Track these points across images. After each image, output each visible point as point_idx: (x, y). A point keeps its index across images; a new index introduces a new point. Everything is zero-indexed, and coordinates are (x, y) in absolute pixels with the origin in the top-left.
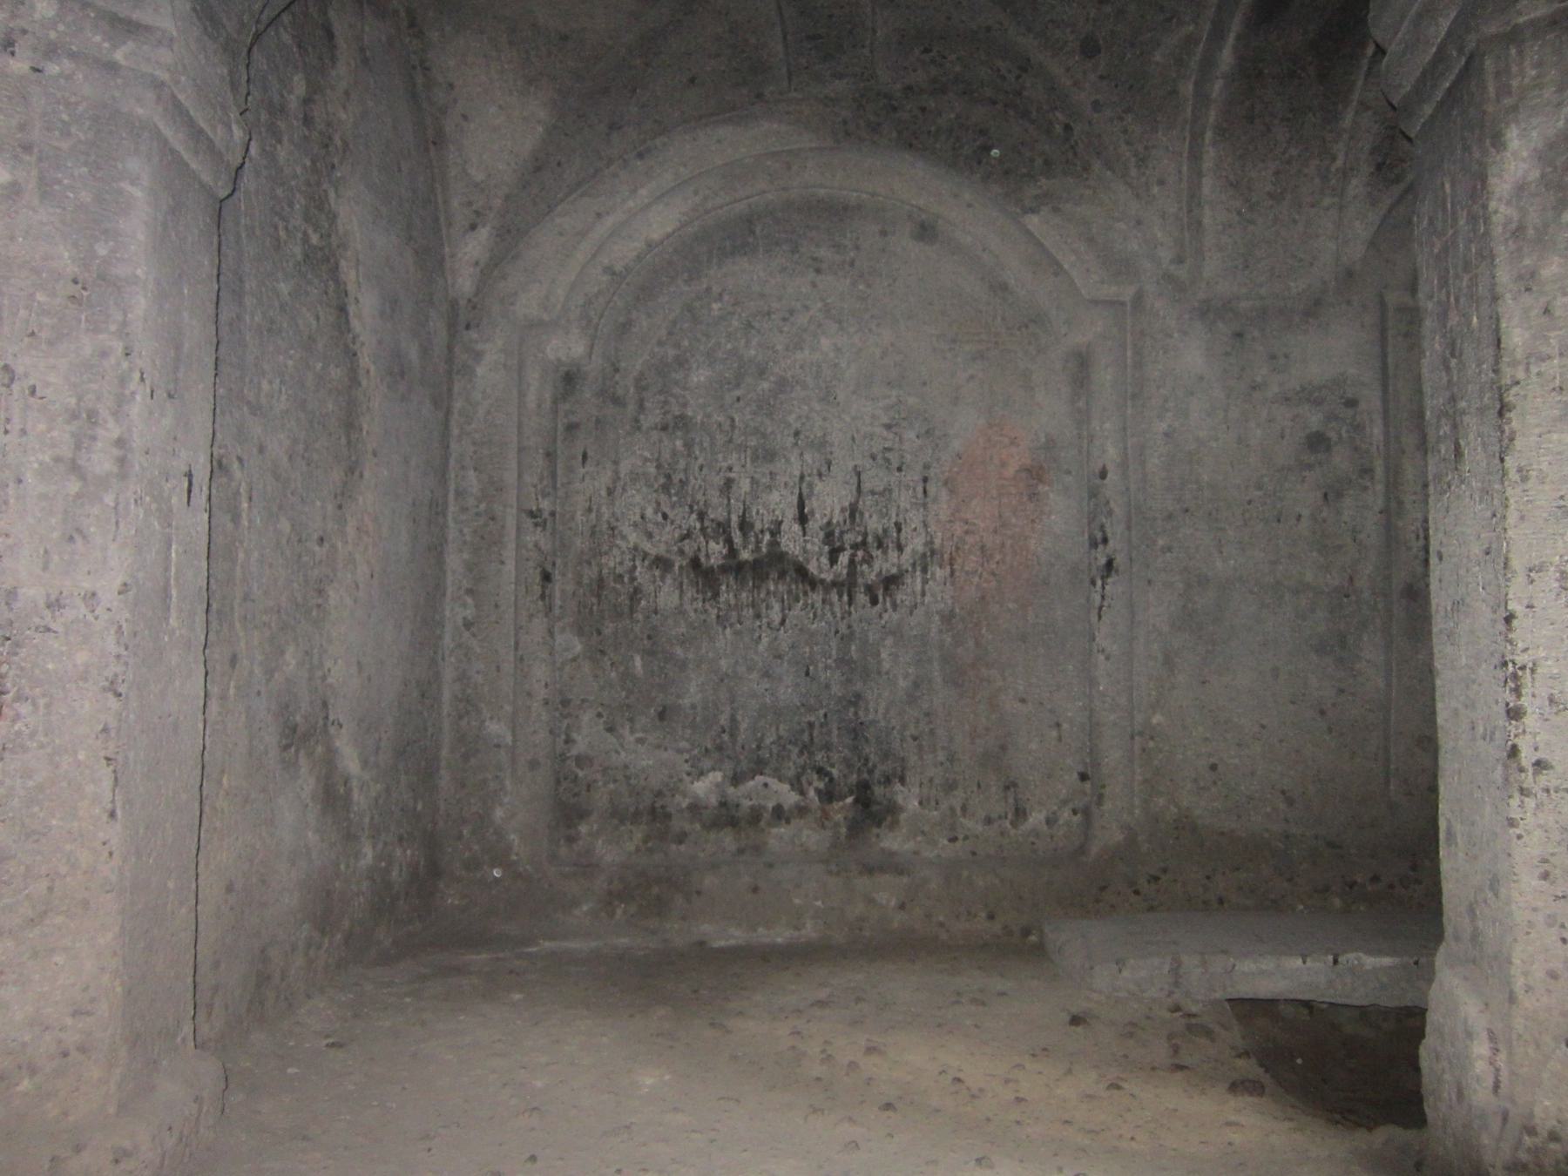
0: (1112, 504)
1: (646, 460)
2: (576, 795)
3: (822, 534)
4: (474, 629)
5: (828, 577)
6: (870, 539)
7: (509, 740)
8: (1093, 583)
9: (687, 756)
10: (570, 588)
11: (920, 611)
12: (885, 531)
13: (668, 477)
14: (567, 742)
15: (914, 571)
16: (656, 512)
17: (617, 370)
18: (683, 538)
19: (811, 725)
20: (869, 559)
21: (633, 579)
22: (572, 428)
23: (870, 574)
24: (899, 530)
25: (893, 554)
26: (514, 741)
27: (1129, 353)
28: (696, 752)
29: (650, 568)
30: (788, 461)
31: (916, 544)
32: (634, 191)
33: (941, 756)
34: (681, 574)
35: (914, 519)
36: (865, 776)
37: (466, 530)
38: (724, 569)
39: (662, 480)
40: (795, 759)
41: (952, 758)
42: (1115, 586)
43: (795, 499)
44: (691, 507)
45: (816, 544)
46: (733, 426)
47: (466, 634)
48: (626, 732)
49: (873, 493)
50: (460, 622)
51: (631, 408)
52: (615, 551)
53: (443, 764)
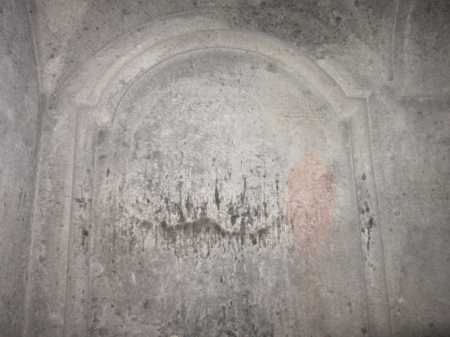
0: (370, 192)
1: (139, 173)
3: (227, 209)
4: (44, 262)
5: (231, 230)
6: (251, 211)
7: (62, 322)
8: (363, 231)
9: (159, 327)
10: (99, 238)
11: (278, 247)
13: (150, 181)
14: (94, 321)
15: (274, 227)
16: (144, 199)
17: (125, 130)
18: (157, 212)
19: (224, 308)
20: (251, 221)
21: (132, 233)
22: (102, 157)
23: (252, 229)
24: (266, 206)
25: (263, 218)
26: (65, 323)
27: (370, 122)
28: (164, 325)
29: (140, 227)
30: (210, 173)
31: (274, 213)
32: (135, 46)
33: (292, 322)
34: (156, 230)
35: (273, 200)
36: (253, 334)
37: (43, 209)
38: (178, 227)
39: (147, 183)
41: (297, 324)
43: (214, 192)
44: (161, 196)
45: (224, 214)
46: (182, 156)
47: (41, 265)
48: (127, 315)
49: (252, 188)
50: (38, 258)
51: (132, 148)
52: (123, 219)
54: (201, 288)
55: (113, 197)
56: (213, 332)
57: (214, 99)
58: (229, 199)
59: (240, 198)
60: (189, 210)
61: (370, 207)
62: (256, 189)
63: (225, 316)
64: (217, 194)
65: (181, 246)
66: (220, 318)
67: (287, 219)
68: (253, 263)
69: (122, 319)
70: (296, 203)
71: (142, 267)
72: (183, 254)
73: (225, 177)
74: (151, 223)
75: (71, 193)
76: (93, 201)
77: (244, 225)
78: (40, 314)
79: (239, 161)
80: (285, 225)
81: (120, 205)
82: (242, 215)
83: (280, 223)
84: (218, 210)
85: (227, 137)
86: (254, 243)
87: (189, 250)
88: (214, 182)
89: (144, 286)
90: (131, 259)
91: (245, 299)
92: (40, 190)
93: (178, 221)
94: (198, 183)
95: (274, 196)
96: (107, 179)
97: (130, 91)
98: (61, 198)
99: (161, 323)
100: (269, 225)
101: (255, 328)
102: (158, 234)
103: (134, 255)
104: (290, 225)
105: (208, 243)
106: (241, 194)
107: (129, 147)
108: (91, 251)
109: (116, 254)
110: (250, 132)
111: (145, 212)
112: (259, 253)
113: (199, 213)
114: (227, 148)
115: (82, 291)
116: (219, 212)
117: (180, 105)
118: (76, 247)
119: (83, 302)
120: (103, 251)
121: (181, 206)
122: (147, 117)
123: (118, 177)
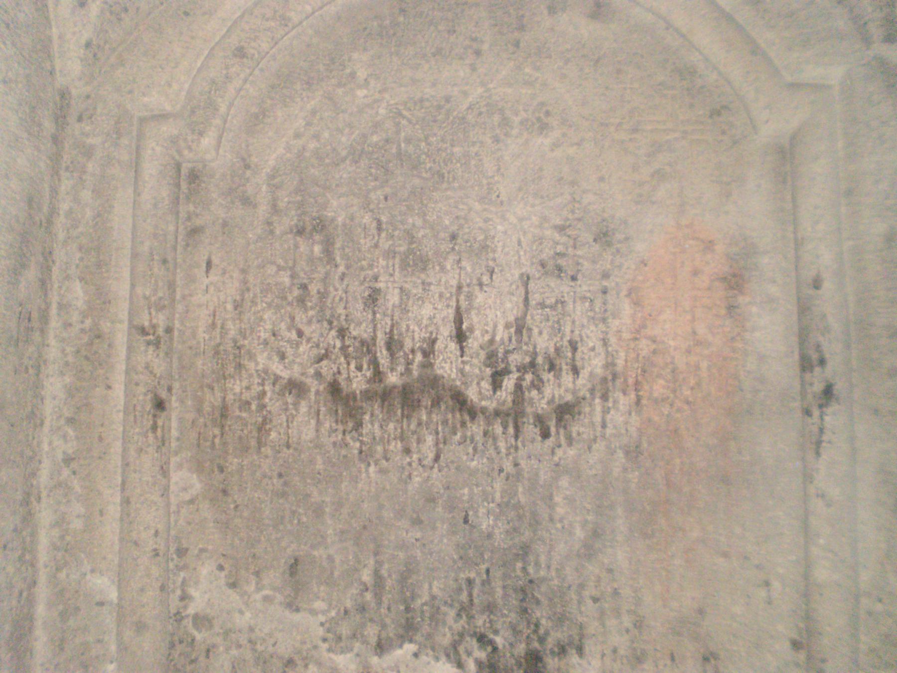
1: (280, 268)
2: (193, 662)
3: (483, 355)
4: (74, 465)
5: (490, 405)
6: (540, 360)
7: (113, 595)
9: (322, 618)
10: (190, 416)
11: (600, 446)
12: (557, 350)
13: (304, 287)
14: (182, 598)
15: (593, 399)
16: (289, 329)
17: (247, 167)
19: (470, 582)
20: (538, 384)
21: (262, 407)
22: (194, 232)
23: (540, 402)
24: (574, 349)
25: (567, 379)
26: (120, 599)
28: (333, 613)
29: (281, 394)
30: (443, 269)
31: (594, 365)
34: (317, 402)
35: (592, 336)
36: (536, 645)
38: (368, 396)
39: (296, 292)
40: (452, 622)
41: (639, 624)
42: (834, 417)
43: (451, 313)
44: (330, 323)
45: (475, 366)
47: (66, 472)
50: (60, 456)
51: (263, 210)
53: (39, 623)
54: (419, 535)
55: (219, 323)
56: (445, 635)
57: (455, 89)
58: (487, 332)
59: (513, 330)
60: (392, 355)
61: (827, 356)
62: (553, 307)
63: (472, 600)
64: (459, 320)
65: (374, 438)
66: (461, 603)
67: (626, 381)
68: (541, 483)
69: (242, 596)
70: (649, 343)
71: (285, 484)
72: (378, 456)
73: (479, 279)
74: (305, 384)
75: (126, 313)
76: (176, 333)
77: (523, 393)
78: (68, 576)
79: (514, 239)
80: (621, 395)
81: (235, 341)
82: (518, 371)
83: (608, 390)
84: (462, 356)
85: (485, 182)
86: (545, 435)
87: (392, 447)
88: (454, 290)
89: (289, 527)
90: (260, 466)
91: (519, 565)
92: (60, 306)
93: (368, 382)
94: (415, 291)
95: (596, 326)
96: (206, 281)
97: (257, 72)
98: (105, 326)
99: (328, 611)
100: (581, 394)
101: (542, 631)
102: (323, 409)
103: (267, 457)
104: (633, 396)
105: (437, 433)
106: (517, 319)
107: (255, 206)
108: (174, 444)
109: (226, 452)
110: (541, 169)
111: (291, 358)
112: (556, 459)
113: (415, 364)
114: (485, 210)
115: (153, 531)
116: (463, 362)
117: (375, 106)
118: (138, 434)
119: (157, 555)
120: (199, 445)
121: (375, 345)
122: (297, 136)
123: (231, 277)
